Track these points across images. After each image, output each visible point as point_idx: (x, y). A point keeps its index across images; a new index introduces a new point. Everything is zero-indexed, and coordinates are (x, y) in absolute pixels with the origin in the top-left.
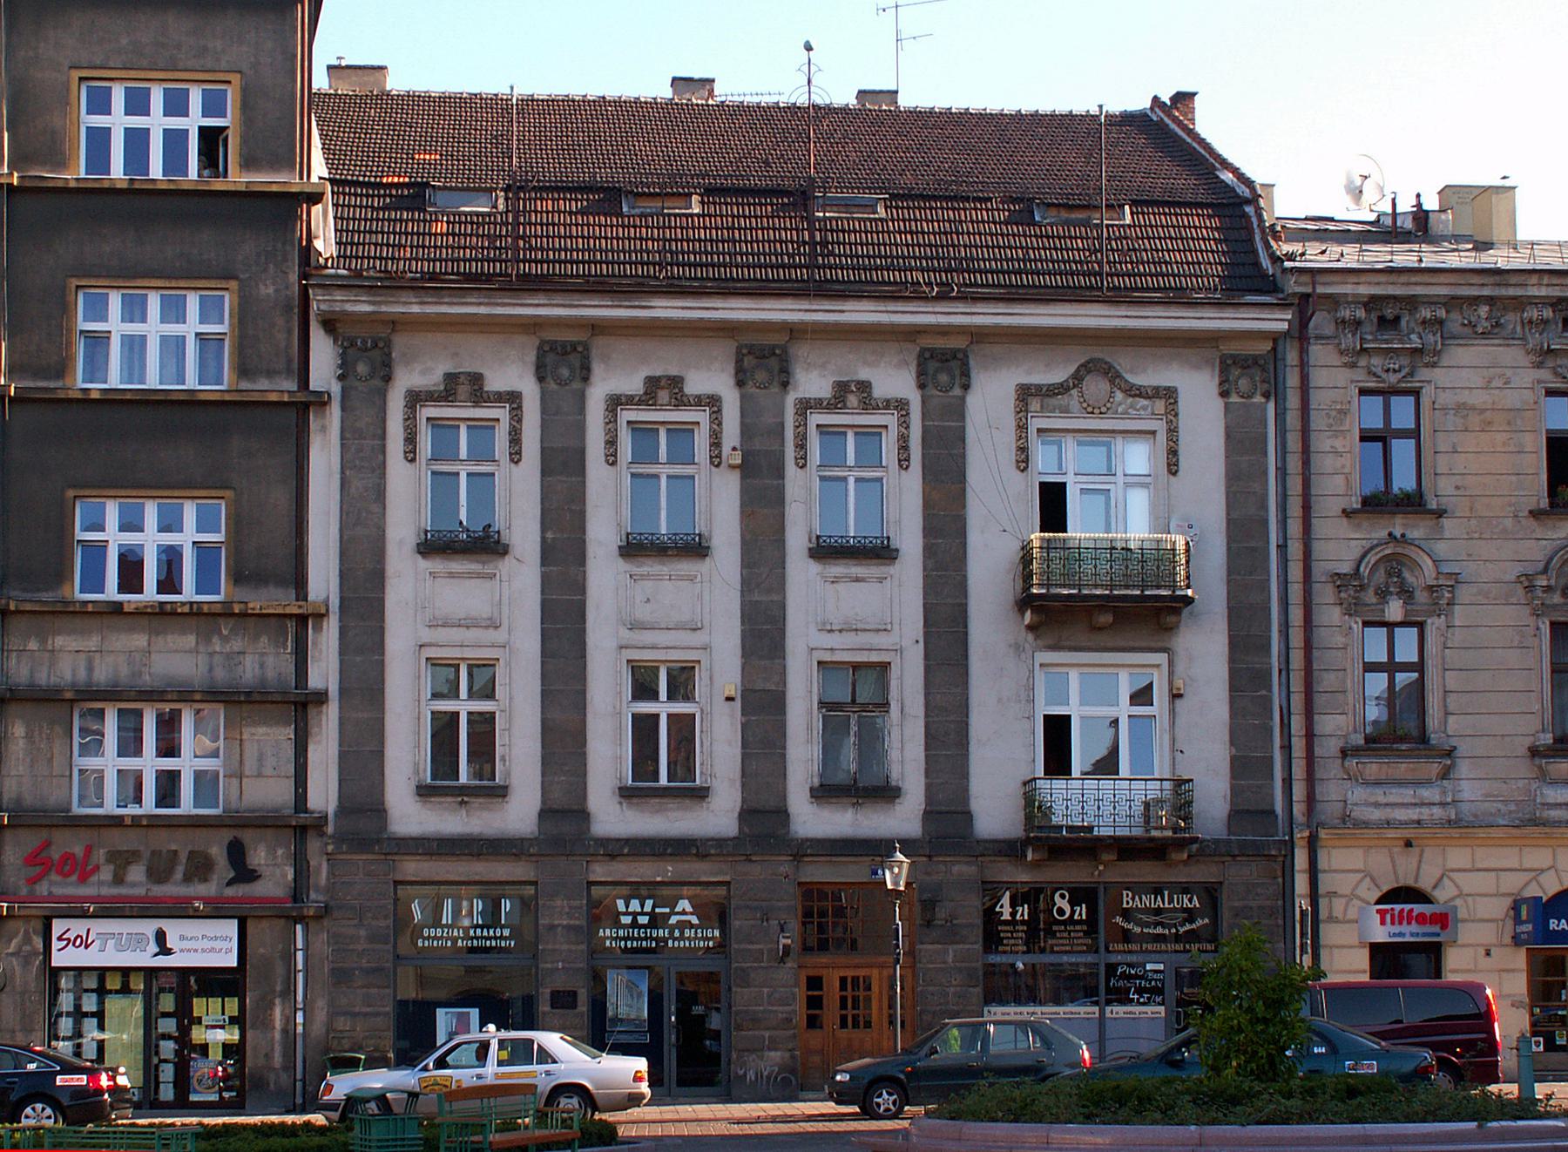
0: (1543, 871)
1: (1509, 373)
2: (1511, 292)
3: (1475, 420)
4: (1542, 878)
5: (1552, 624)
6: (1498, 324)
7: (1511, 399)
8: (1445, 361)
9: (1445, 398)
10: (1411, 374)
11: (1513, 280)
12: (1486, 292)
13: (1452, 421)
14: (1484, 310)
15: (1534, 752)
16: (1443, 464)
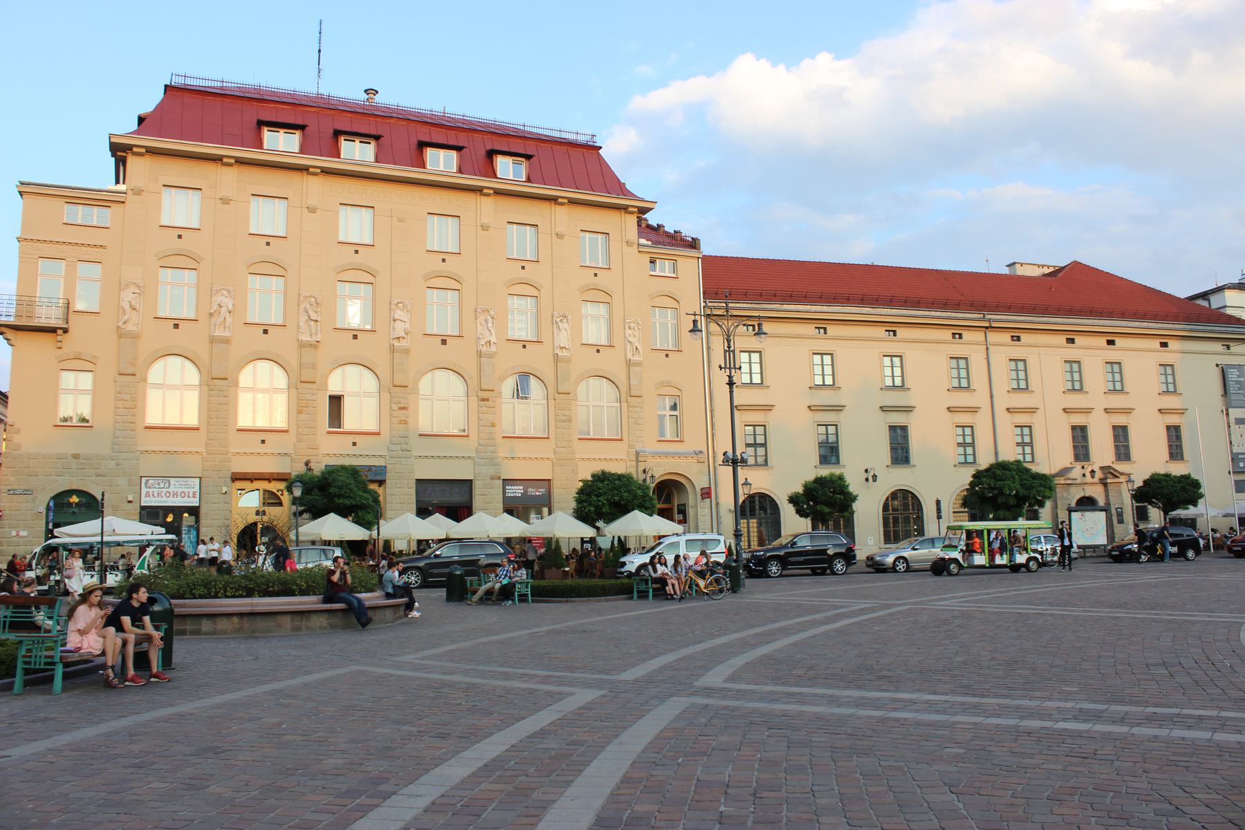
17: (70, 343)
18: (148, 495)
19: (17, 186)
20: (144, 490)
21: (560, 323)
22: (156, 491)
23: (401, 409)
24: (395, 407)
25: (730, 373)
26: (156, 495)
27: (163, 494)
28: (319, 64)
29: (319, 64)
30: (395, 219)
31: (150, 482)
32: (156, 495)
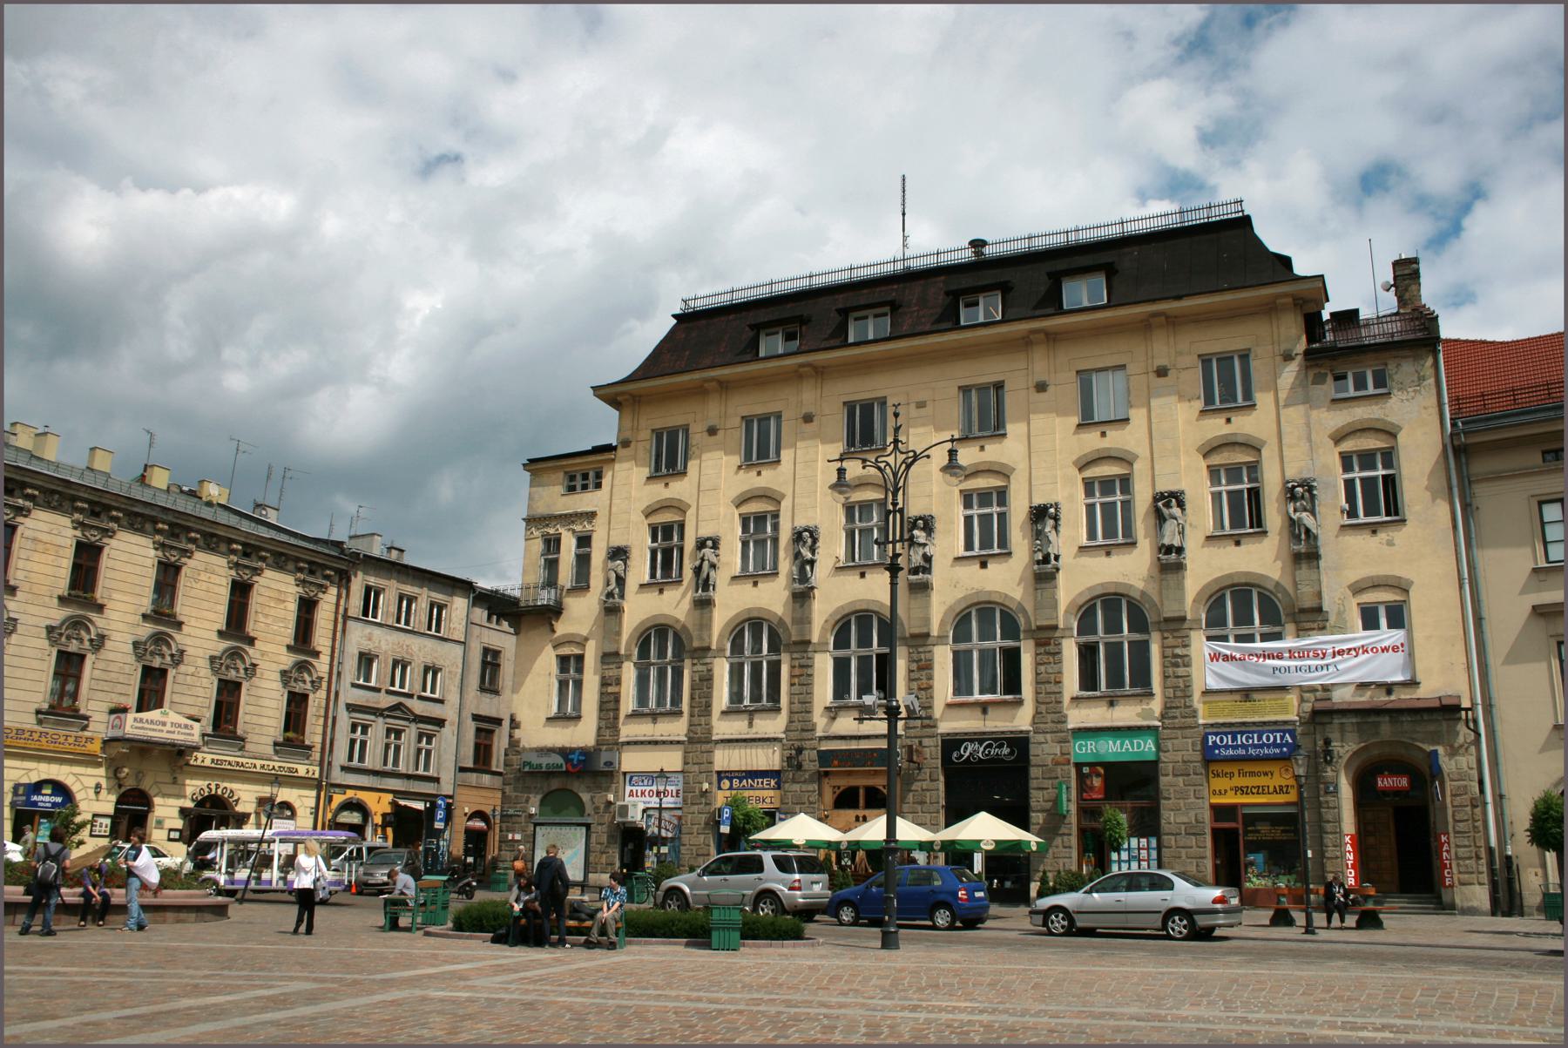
0: (31, 770)
1: (62, 528)
2: (72, 492)
3: (40, 547)
4: (30, 774)
5: (59, 651)
6: (61, 505)
7: (59, 541)
8: (32, 516)
9: (28, 533)
10: (14, 518)
11: (74, 487)
12: (59, 489)
13: (29, 544)
14: (56, 497)
15: (38, 712)
16: (21, 564)
17: (562, 628)
18: (631, 794)
19: (524, 465)
20: (628, 788)
21: (1165, 511)
22: (639, 789)
23: (920, 669)
24: (914, 667)
25: (894, 549)
26: (639, 794)
27: (647, 793)
28: (904, 230)
29: (904, 230)
30: (913, 406)
31: (634, 779)
32: (639, 794)
